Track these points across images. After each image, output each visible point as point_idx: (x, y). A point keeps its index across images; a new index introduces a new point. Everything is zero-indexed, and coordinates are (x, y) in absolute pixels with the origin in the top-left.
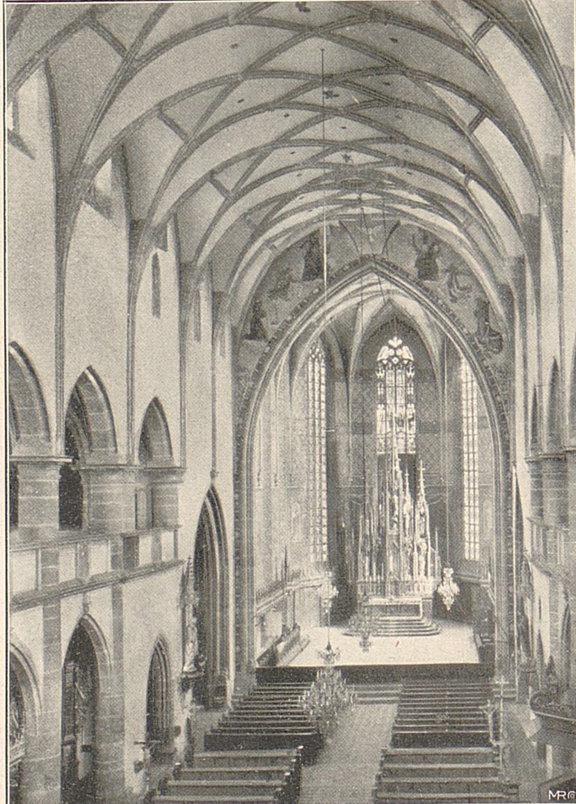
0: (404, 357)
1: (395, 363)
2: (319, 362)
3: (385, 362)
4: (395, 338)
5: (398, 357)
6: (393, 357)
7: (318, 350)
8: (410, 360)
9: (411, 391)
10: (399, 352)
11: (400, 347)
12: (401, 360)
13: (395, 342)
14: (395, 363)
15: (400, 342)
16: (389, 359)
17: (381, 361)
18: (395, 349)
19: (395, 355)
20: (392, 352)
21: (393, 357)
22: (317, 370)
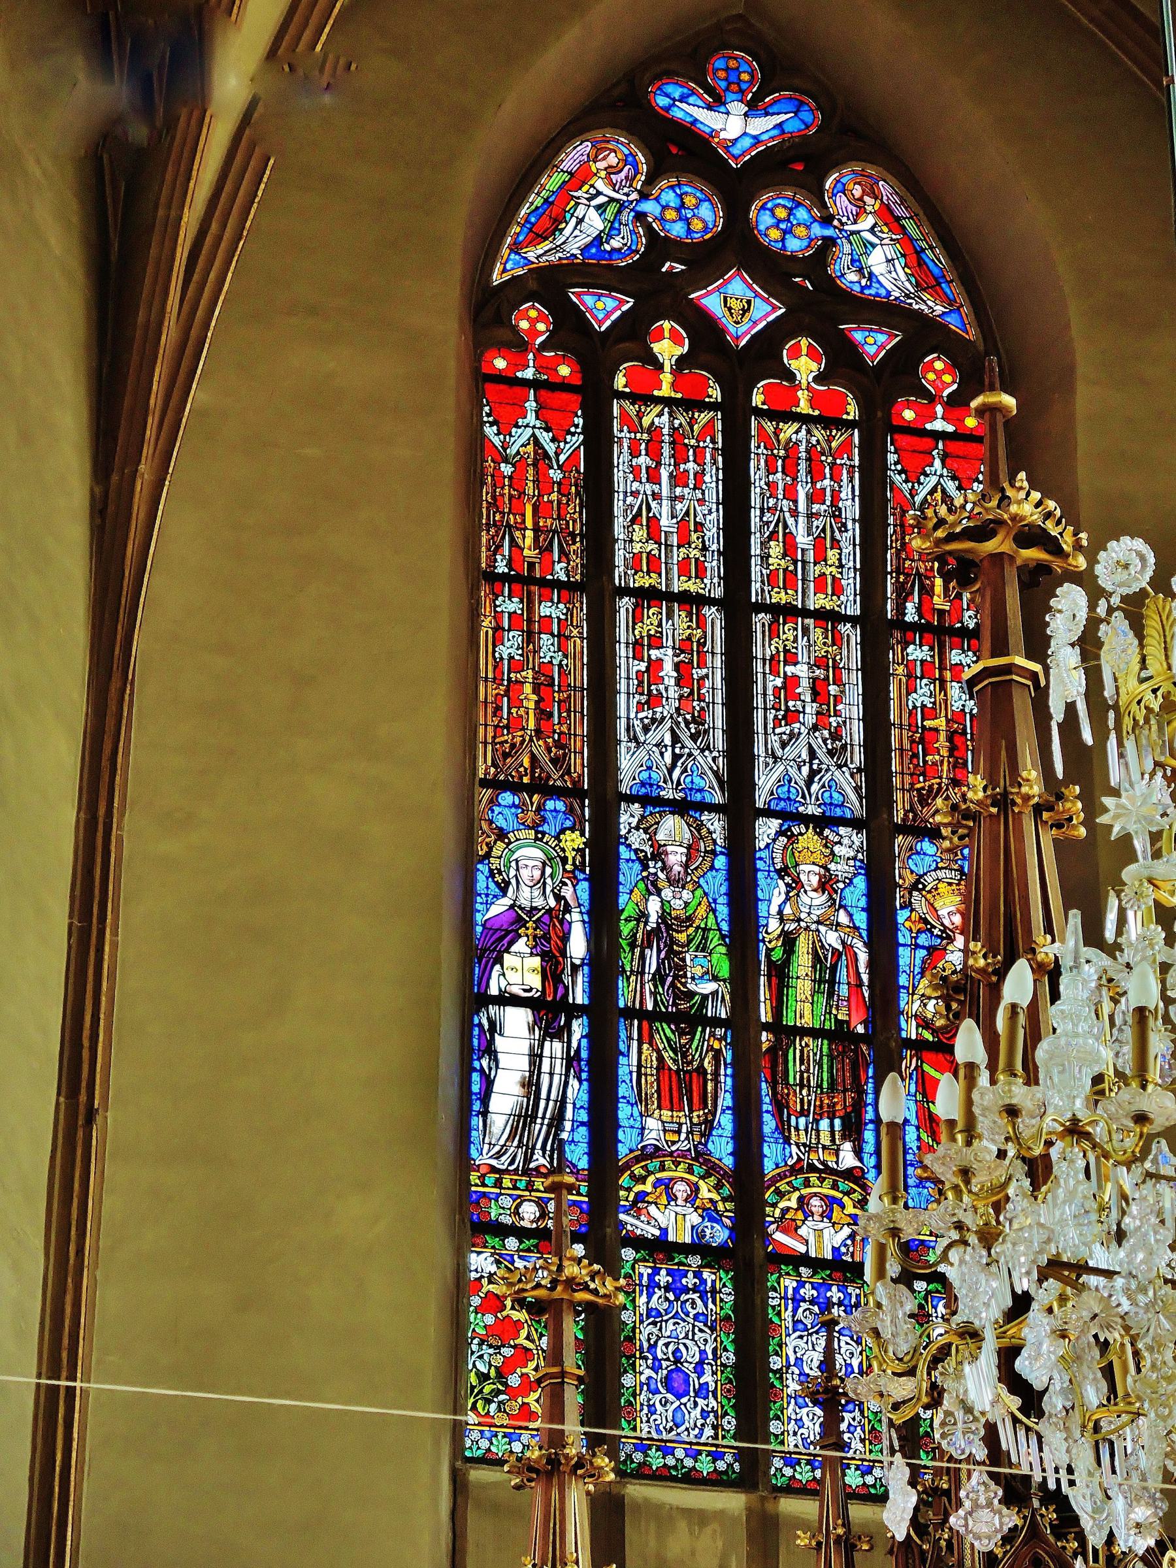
1: (741, 332)
14: (741, 332)
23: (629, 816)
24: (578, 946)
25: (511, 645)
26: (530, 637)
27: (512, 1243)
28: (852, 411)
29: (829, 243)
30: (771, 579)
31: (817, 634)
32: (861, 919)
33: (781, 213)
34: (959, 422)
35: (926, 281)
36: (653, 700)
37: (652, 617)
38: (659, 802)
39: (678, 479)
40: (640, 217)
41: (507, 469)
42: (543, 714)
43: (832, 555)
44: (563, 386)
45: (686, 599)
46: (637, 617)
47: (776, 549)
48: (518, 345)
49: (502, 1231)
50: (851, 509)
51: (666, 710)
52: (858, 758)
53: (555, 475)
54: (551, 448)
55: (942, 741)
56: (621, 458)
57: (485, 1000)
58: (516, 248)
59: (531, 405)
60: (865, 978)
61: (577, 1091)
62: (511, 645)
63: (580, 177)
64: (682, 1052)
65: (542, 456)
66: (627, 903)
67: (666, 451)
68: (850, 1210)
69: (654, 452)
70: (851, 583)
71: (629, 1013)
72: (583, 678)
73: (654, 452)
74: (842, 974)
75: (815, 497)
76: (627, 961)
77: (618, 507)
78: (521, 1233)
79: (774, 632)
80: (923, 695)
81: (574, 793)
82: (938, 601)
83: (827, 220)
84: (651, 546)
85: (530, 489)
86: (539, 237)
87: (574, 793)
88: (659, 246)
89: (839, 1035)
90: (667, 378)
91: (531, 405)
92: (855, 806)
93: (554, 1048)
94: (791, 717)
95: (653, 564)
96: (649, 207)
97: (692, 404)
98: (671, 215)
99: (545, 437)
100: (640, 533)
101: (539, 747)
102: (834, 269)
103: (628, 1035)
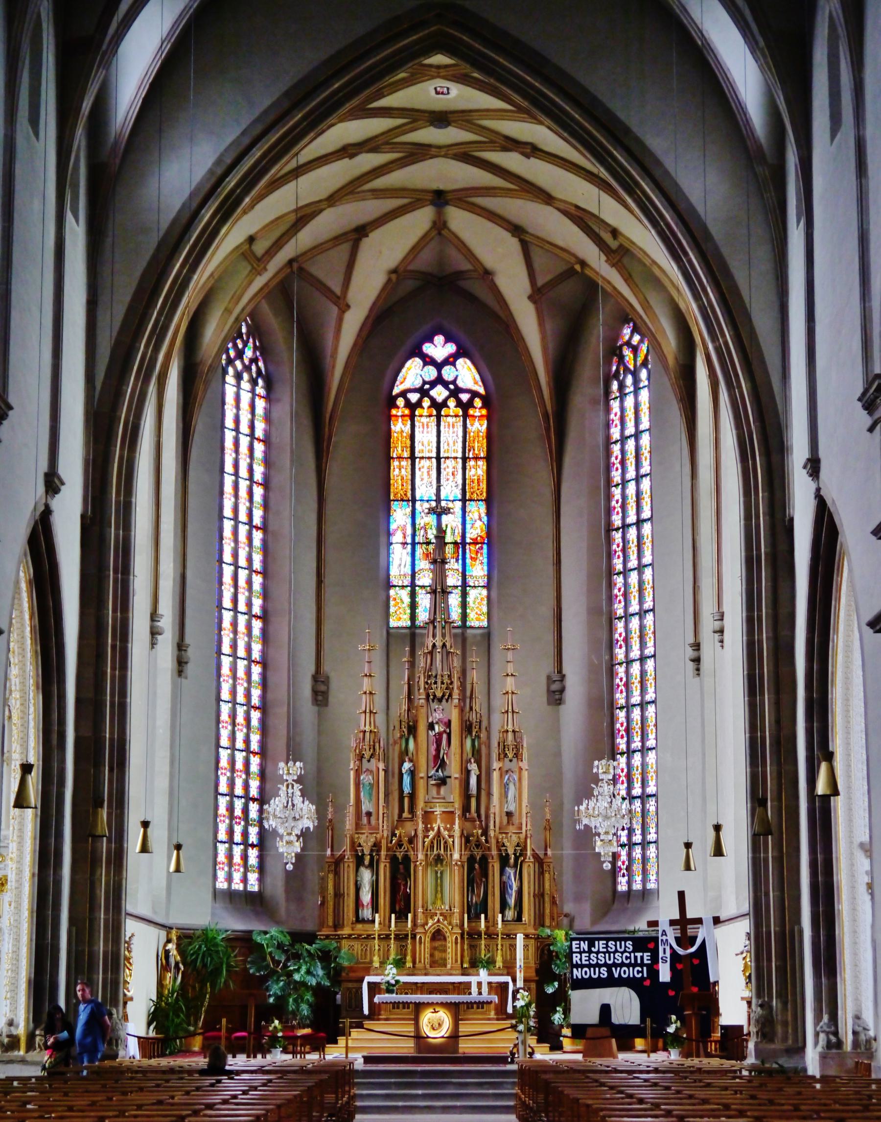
0: (460, 383)
2: (254, 382)
3: (414, 397)
4: (439, 339)
5: (445, 384)
6: (433, 384)
7: (249, 353)
8: (474, 394)
9: (478, 470)
10: (448, 373)
11: (450, 360)
12: (455, 392)
13: (439, 349)
14: (440, 399)
15: (451, 348)
16: (423, 392)
17: (403, 394)
18: (439, 366)
19: (439, 380)
20: (431, 373)
21: (433, 384)
22: (245, 397)
23: (418, 504)
24: (409, 531)
25: (397, 471)
26: (400, 469)
27: (397, 588)
28: (461, 413)
29: (457, 376)
30: (444, 452)
31: (453, 461)
32: (460, 520)
33: (448, 370)
34: (481, 412)
35: (476, 383)
36: (422, 479)
37: (423, 461)
38: (423, 500)
39: (428, 432)
40: (421, 376)
41: (396, 435)
42: (403, 485)
43: (456, 444)
44: (406, 416)
45: (430, 458)
46: (419, 463)
47: (446, 444)
48: (398, 407)
49: (395, 586)
50: (461, 434)
51: (425, 481)
52: (460, 487)
53: (405, 434)
54: (403, 429)
55: (476, 481)
56: (417, 429)
57: (392, 544)
58: (397, 386)
59: (400, 420)
60: (460, 531)
61: (409, 559)
62: (397, 472)
63: (409, 369)
64: (427, 549)
65: (402, 431)
66: (417, 522)
67: (425, 426)
68: (456, 575)
69: (423, 428)
70: (460, 450)
71: (419, 543)
72: (410, 477)
73: (423, 428)
74: (456, 531)
75: (454, 432)
76: (417, 533)
77: (416, 440)
78: (399, 586)
79: (445, 463)
80: (473, 471)
81: (408, 500)
82: (476, 452)
83: (457, 370)
84: (423, 448)
85: (400, 438)
86: (402, 383)
87: (408, 500)
88: (425, 383)
89: (455, 543)
90: (426, 410)
91: (400, 420)
92: (460, 497)
93: (405, 551)
94: (448, 480)
95: (422, 451)
96: (423, 373)
97: (430, 416)
98: (427, 374)
99: (403, 427)
100: (420, 444)
101: (402, 492)
102: (457, 382)
103: (418, 547)
